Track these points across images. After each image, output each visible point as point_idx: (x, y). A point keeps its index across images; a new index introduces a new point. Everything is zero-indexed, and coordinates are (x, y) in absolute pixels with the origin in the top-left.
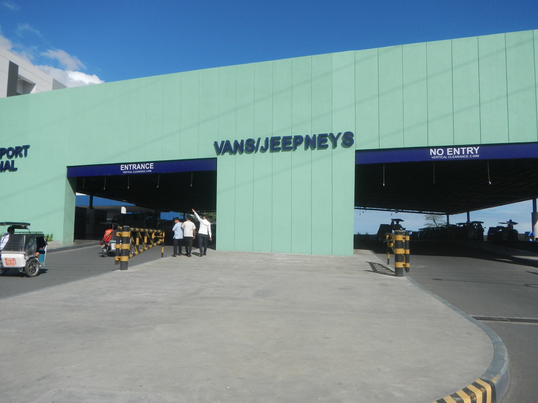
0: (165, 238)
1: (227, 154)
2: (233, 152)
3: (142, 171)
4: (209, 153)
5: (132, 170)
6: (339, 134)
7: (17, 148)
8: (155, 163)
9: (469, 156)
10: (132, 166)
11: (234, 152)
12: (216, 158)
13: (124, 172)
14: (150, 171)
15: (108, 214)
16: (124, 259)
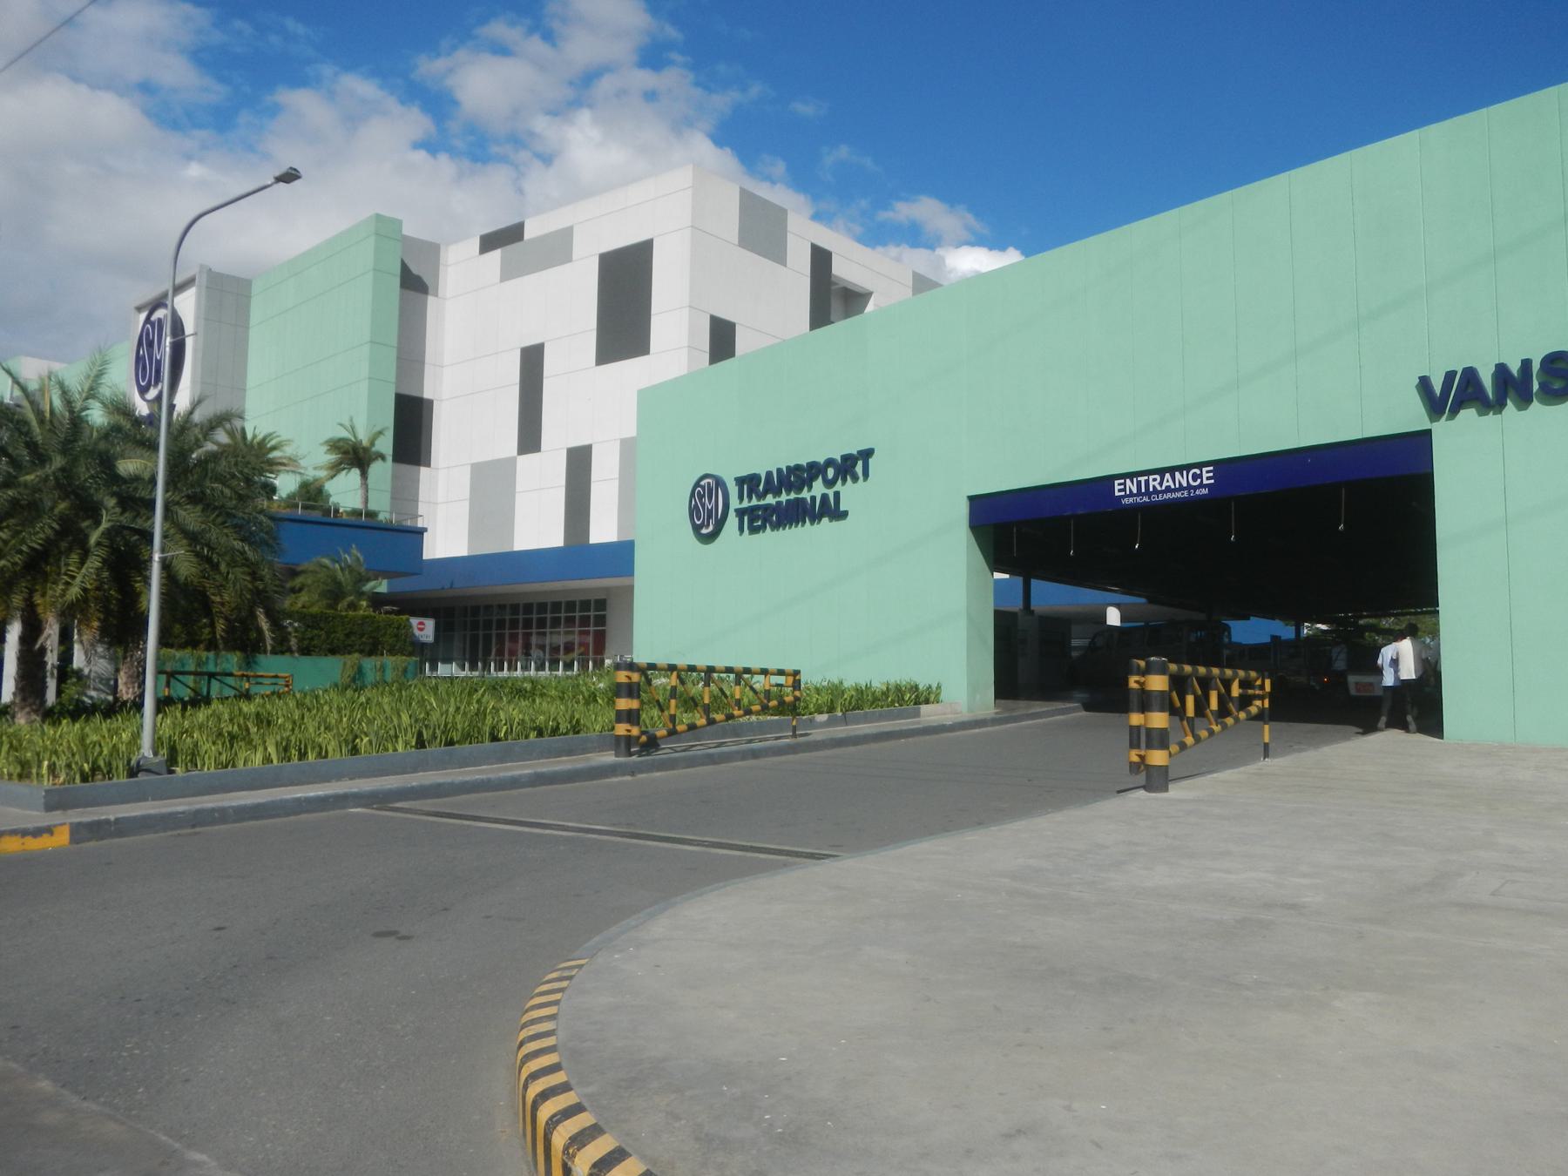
0: (1271, 696)
1: (1468, 415)
2: (1491, 406)
3: (1179, 495)
7: (846, 458)
8: (1217, 464)
10: (1147, 482)
11: (1498, 405)
12: (1428, 433)
13: (1126, 501)
14: (1205, 491)
15: (1075, 629)
16: (1158, 758)
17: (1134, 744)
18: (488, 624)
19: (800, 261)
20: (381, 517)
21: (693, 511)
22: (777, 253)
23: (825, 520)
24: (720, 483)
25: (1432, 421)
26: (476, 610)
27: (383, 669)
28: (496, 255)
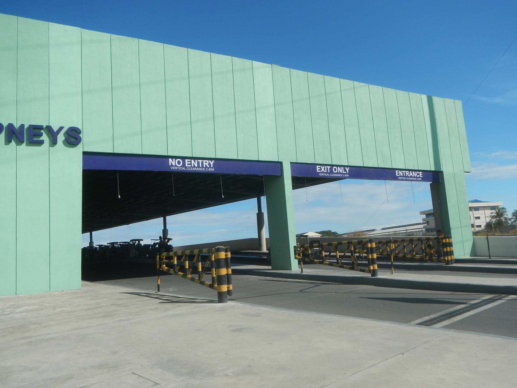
6: (61, 128)
9: (206, 169)
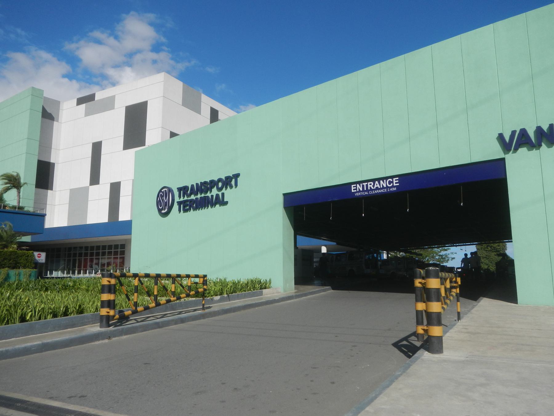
0: (461, 287)
1: (523, 151)
3: (382, 191)
4: (491, 151)
5: (367, 190)
7: (227, 178)
10: (367, 185)
11: (538, 146)
12: (503, 160)
13: (357, 194)
14: (395, 189)
17: (419, 322)
18: (75, 255)
19: (206, 113)
20: (26, 209)
21: (158, 203)
22: (197, 109)
23: (218, 206)
24: (170, 190)
25: (505, 154)
26: (70, 249)
27: (19, 275)
28: (83, 106)
